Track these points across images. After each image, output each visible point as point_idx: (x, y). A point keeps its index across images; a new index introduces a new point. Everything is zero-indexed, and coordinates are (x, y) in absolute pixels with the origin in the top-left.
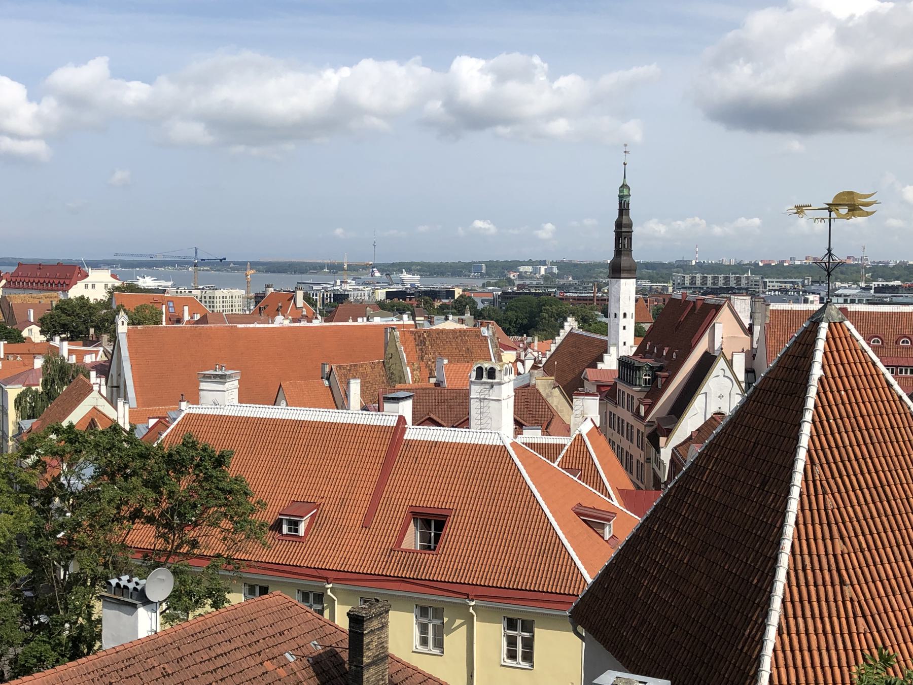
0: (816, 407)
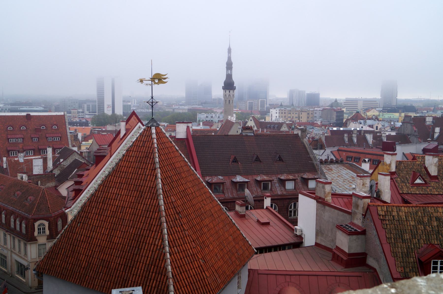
0: (159, 162)
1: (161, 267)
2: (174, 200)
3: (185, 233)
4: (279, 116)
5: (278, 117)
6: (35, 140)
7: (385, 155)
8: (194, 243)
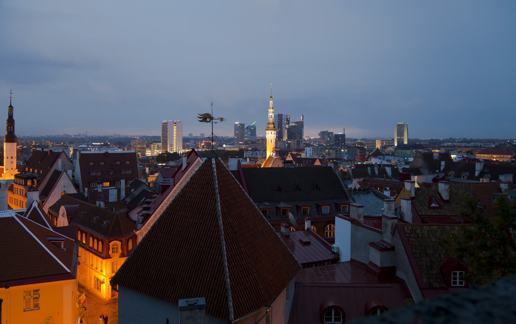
0: (218, 188)
1: (220, 280)
2: (231, 221)
3: (241, 250)
4: (313, 153)
5: (311, 154)
6: (112, 173)
7: (406, 183)
8: (249, 258)
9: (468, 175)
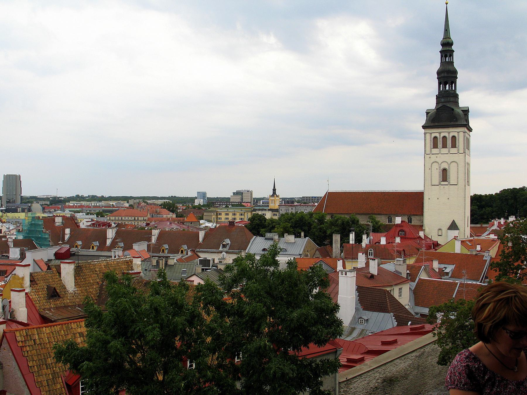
9: (98, 244)
